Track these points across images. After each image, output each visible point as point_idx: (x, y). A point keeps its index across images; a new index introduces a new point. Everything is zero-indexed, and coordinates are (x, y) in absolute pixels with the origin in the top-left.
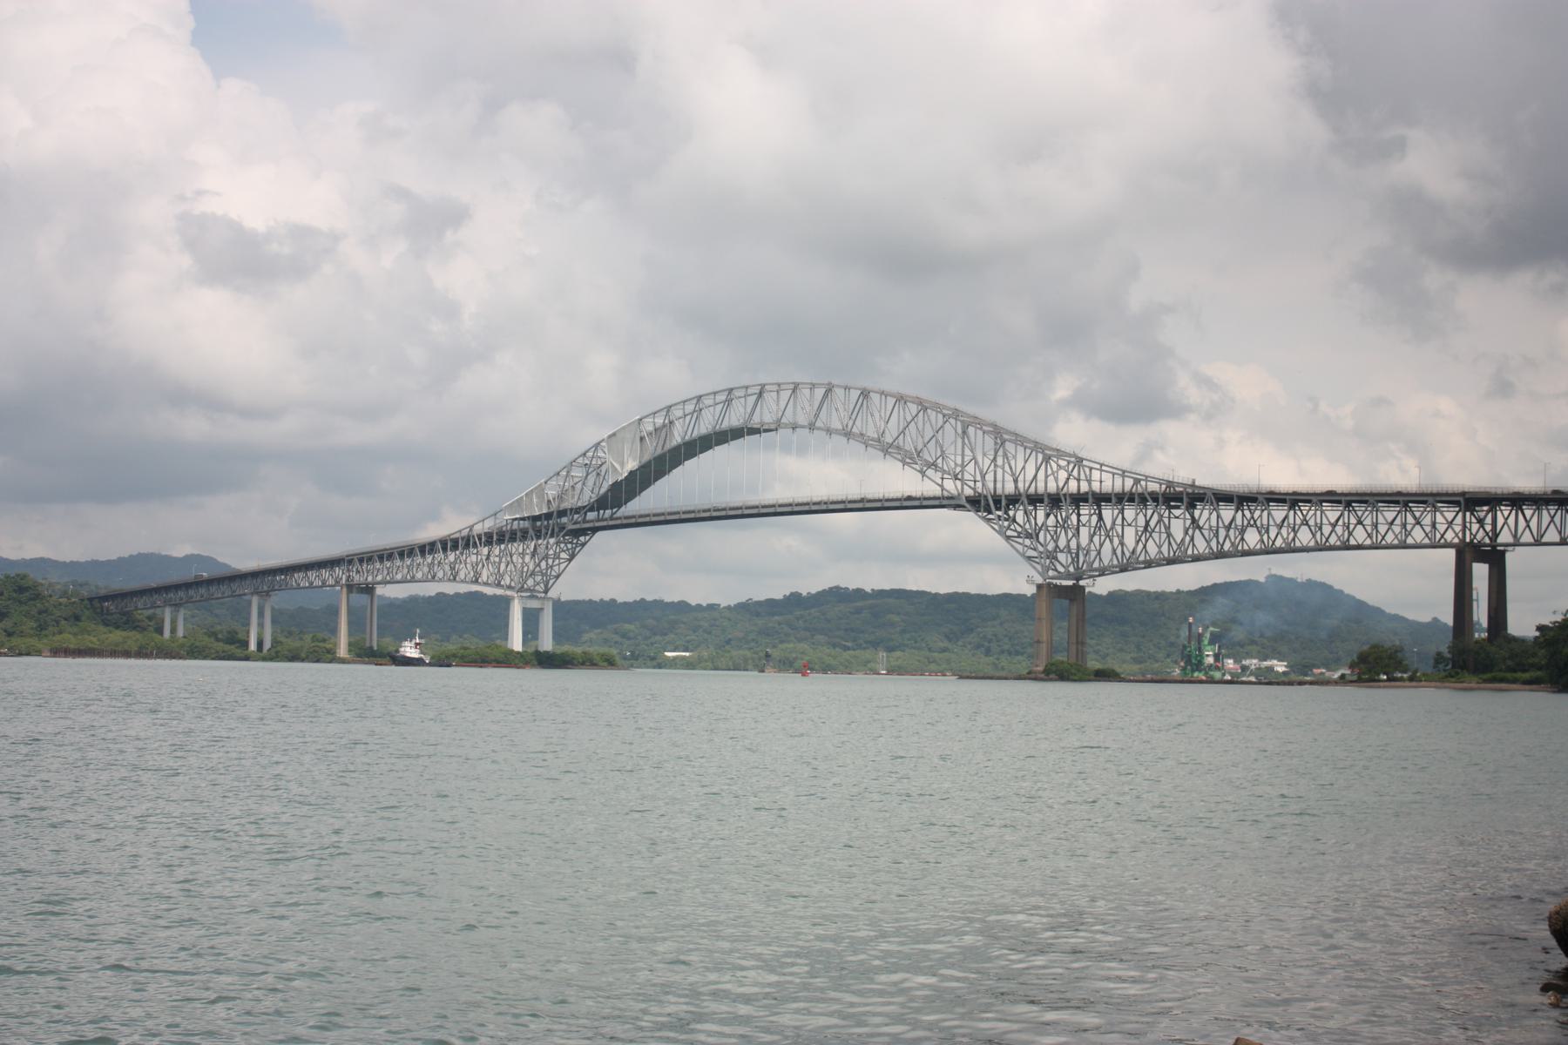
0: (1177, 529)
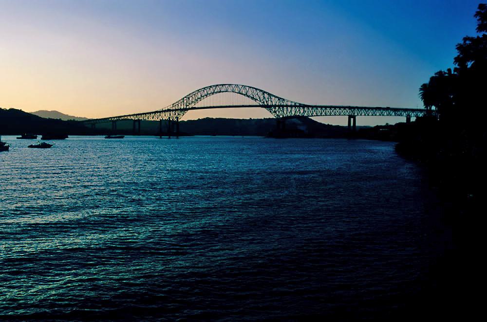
0: (302, 111)
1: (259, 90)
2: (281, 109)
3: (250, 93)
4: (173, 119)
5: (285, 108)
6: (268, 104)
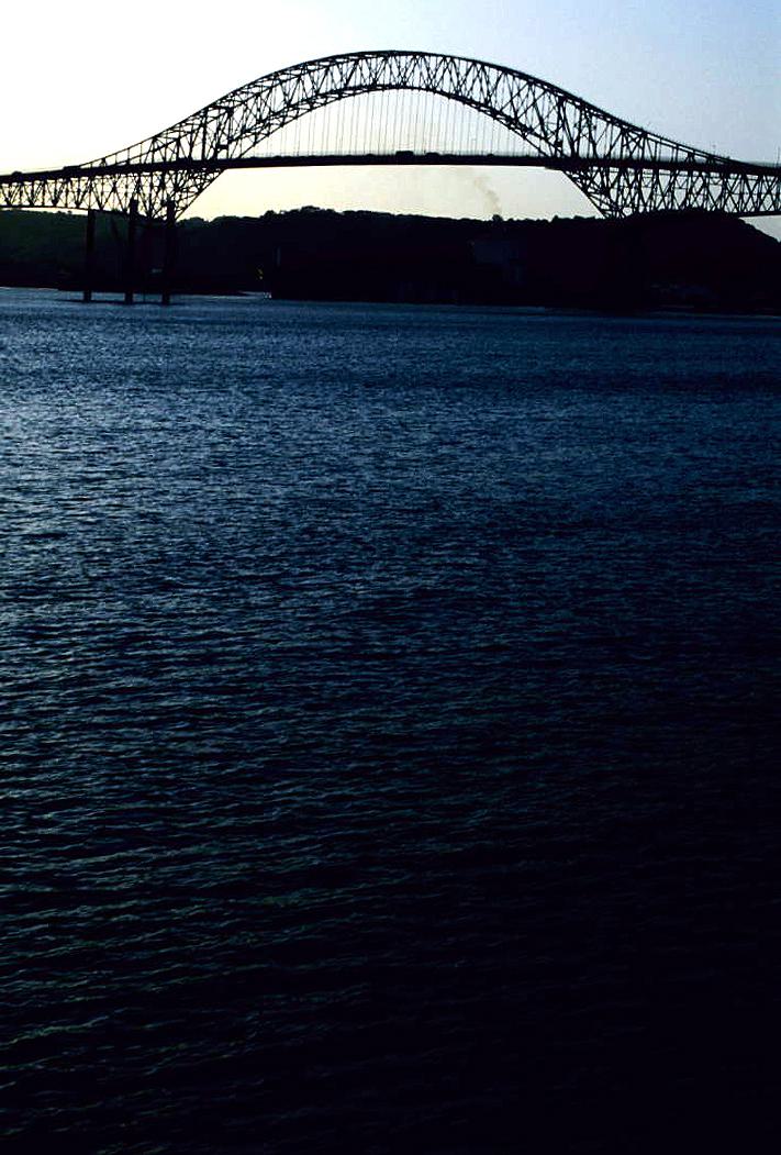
0: (716, 191)
1: (543, 83)
3: (500, 100)
4: (149, 213)
5: (647, 173)
6: (575, 154)
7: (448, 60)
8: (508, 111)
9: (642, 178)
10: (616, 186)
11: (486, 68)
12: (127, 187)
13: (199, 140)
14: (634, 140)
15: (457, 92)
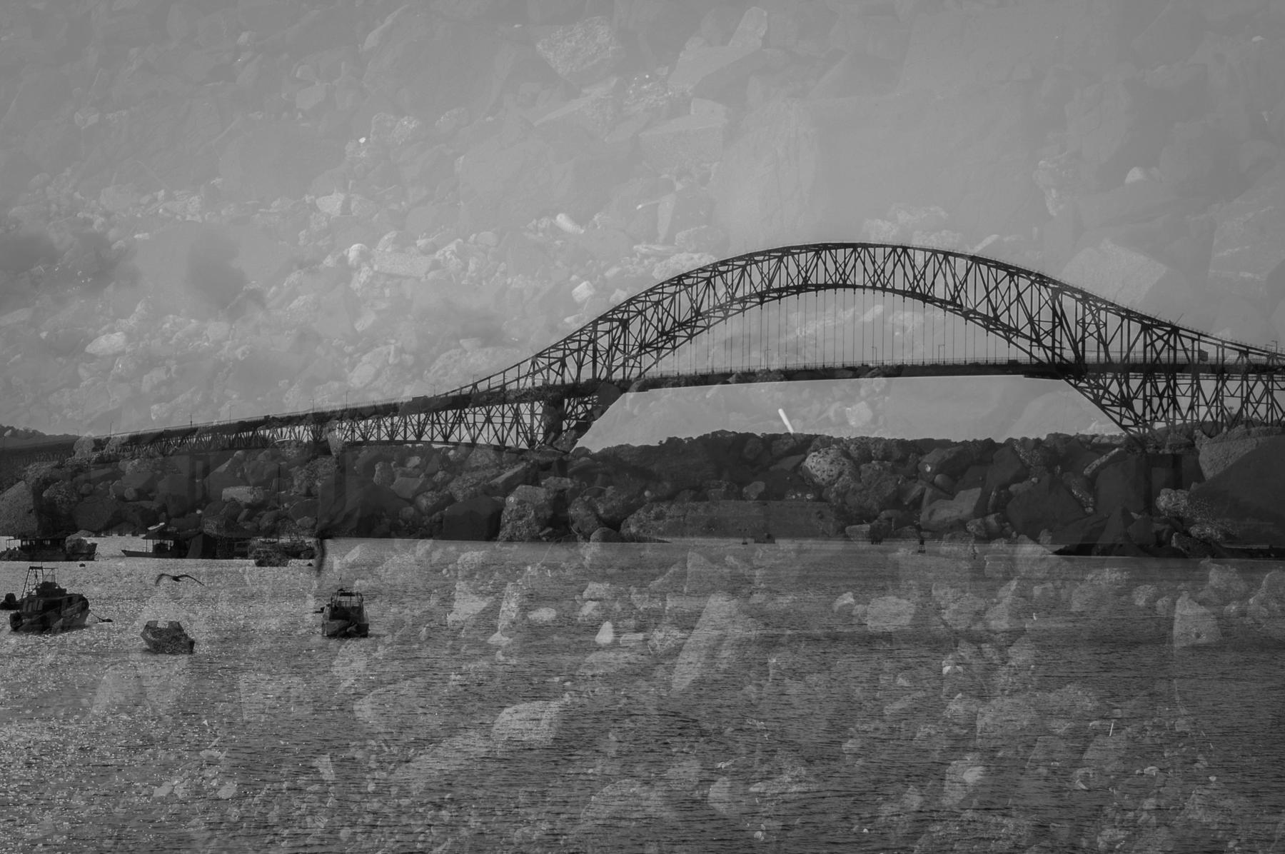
2: (1161, 386)
6: (1080, 358)
7: (900, 251)
8: (982, 309)
9: (1176, 385)
10: (1141, 396)
11: (951, 258)
12: (503, 416)
13: (588, 359)
14: (1160, 337)
15: (914, 289)
